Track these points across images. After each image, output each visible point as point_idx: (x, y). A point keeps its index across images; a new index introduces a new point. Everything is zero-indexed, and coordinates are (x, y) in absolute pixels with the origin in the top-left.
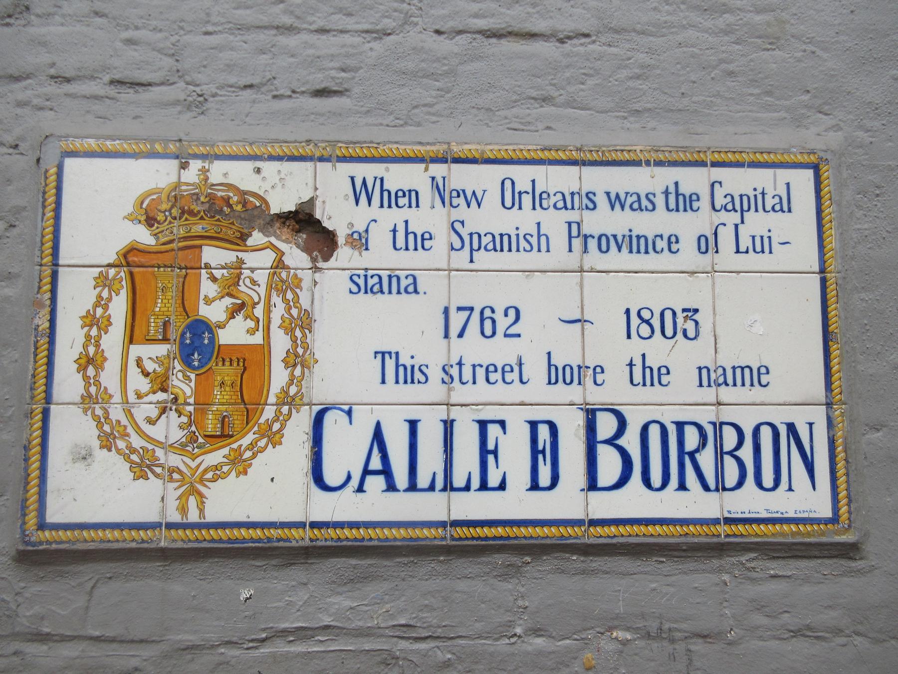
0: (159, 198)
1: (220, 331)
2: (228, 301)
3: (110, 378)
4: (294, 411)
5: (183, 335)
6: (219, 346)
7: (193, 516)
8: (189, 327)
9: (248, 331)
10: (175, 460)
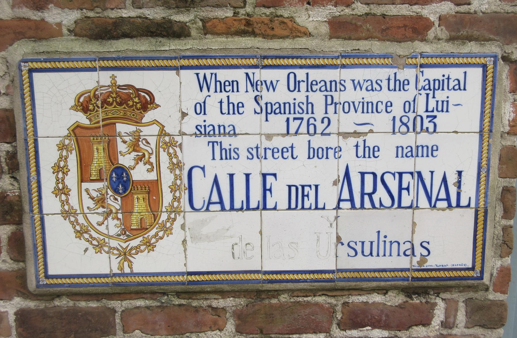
0: (89, 96)
1: (132, 172)
2: (134, 154)
3: (74, 201)
4: (177, 215)
5: (111, 175)
6: (133, 181)
7: (127, 270)
8: (113, 171)
9: (147, 170)
10: (114, 243)
